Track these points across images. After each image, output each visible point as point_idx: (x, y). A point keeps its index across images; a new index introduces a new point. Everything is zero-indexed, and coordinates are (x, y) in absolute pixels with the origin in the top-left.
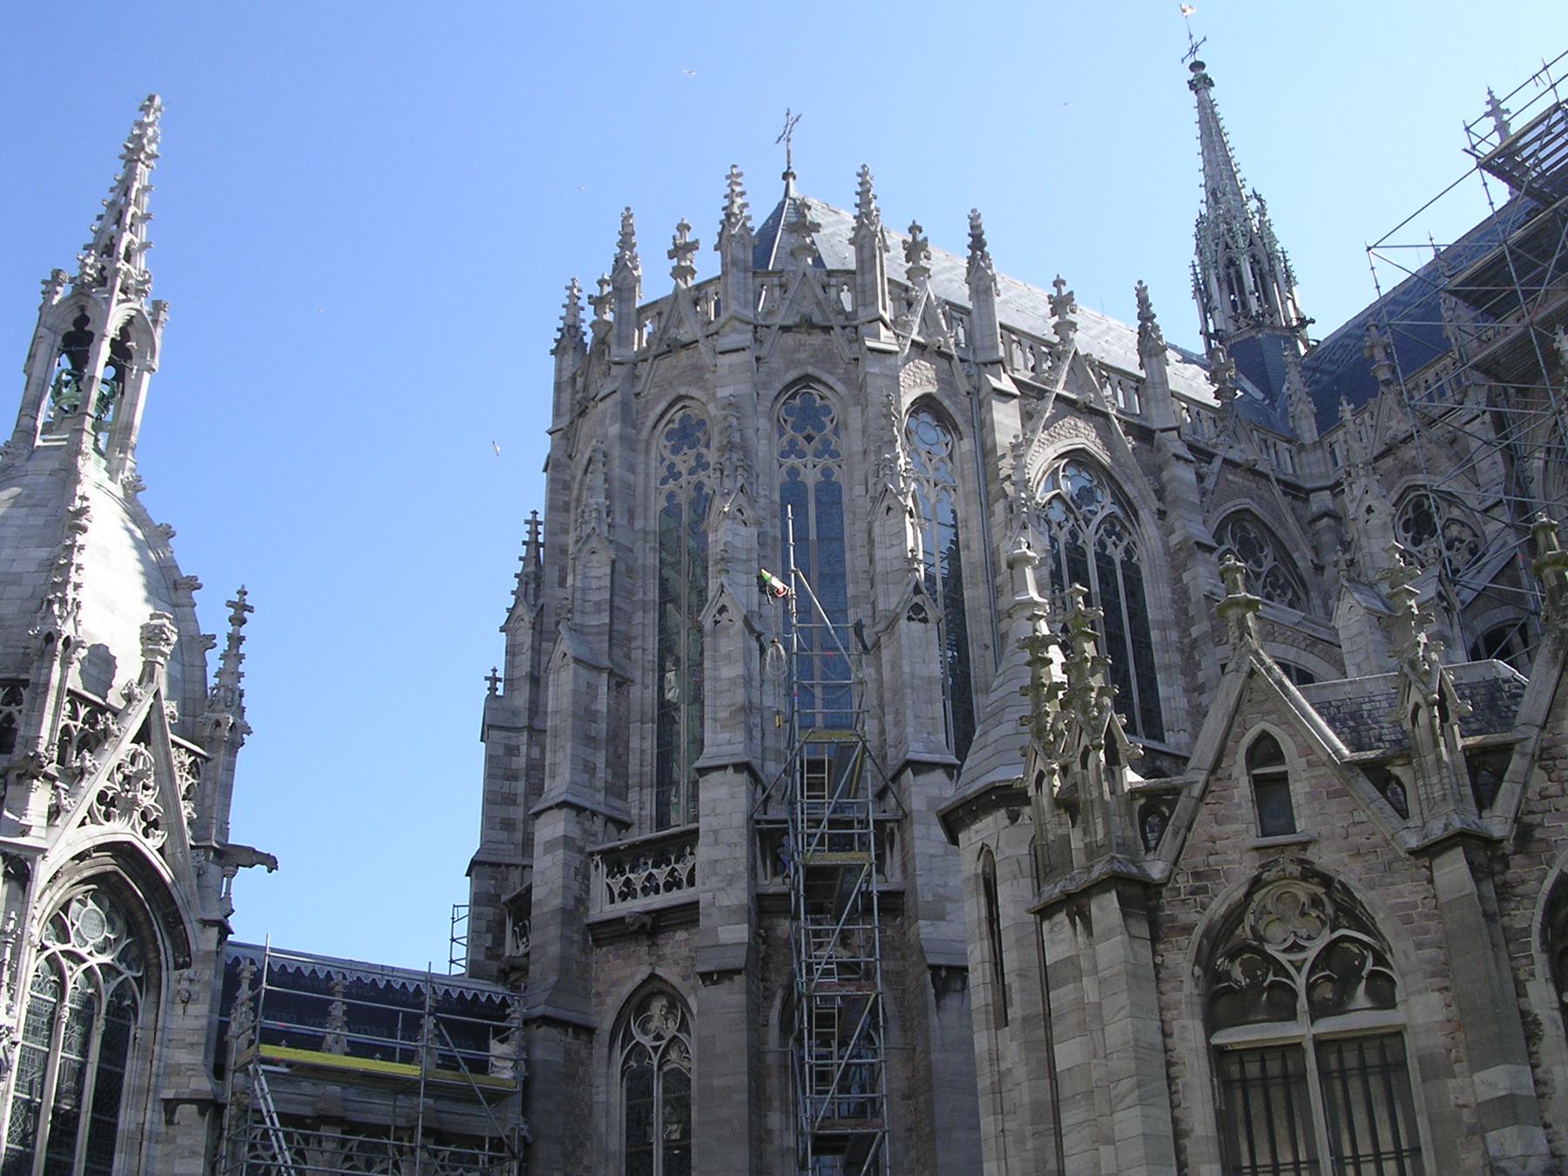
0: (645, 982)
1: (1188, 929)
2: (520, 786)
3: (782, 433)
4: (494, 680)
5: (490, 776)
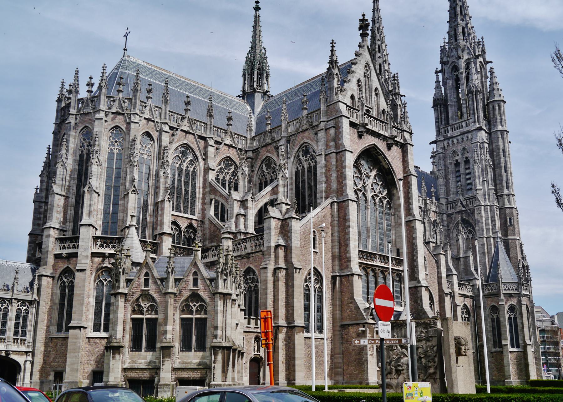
0: (66, 268)
1: (130, 301)
2: (42, 216)
3: (110, 139)
4: (37, 189)
5: (35, 213)
